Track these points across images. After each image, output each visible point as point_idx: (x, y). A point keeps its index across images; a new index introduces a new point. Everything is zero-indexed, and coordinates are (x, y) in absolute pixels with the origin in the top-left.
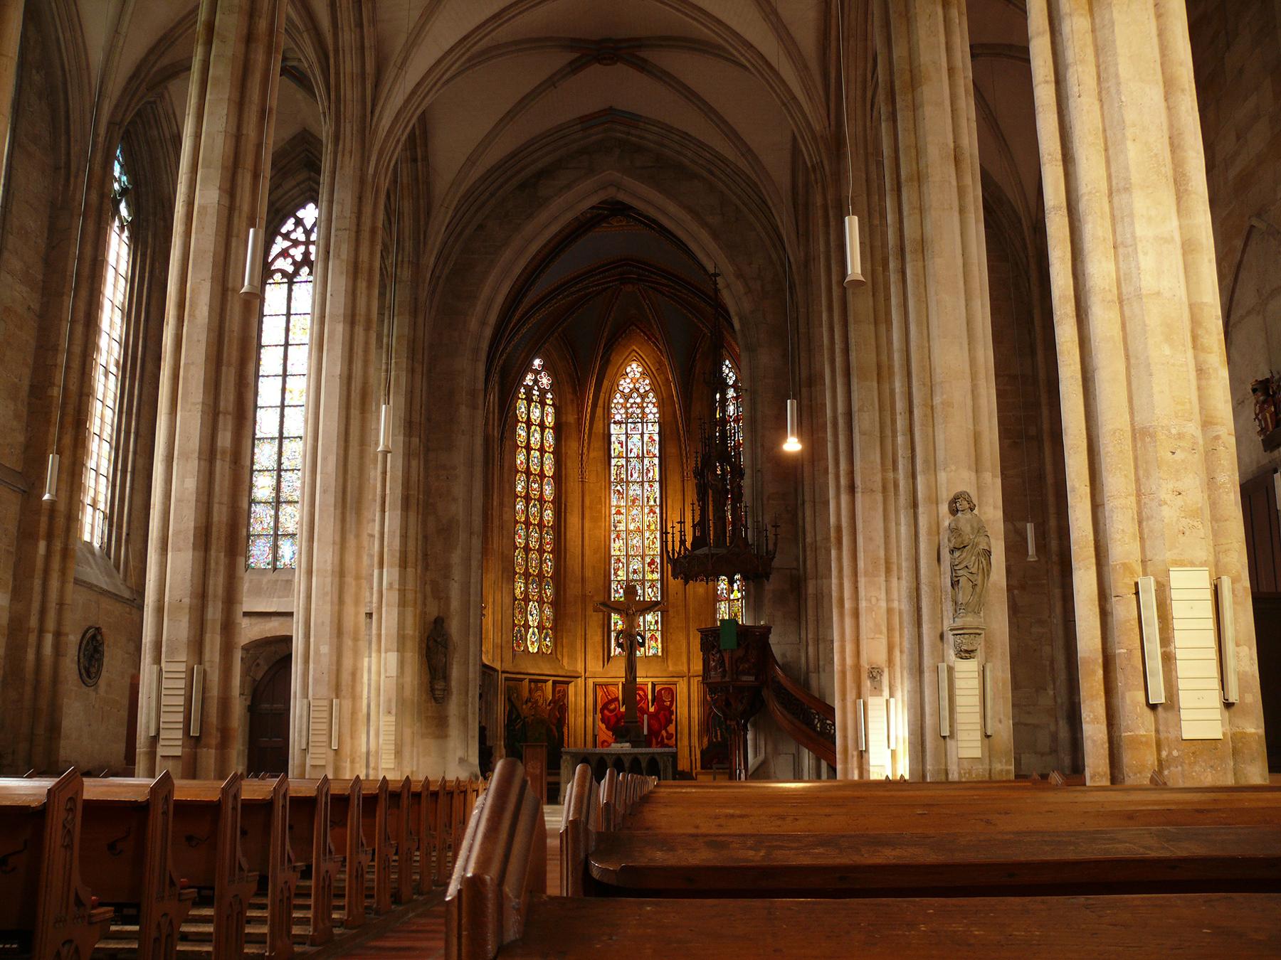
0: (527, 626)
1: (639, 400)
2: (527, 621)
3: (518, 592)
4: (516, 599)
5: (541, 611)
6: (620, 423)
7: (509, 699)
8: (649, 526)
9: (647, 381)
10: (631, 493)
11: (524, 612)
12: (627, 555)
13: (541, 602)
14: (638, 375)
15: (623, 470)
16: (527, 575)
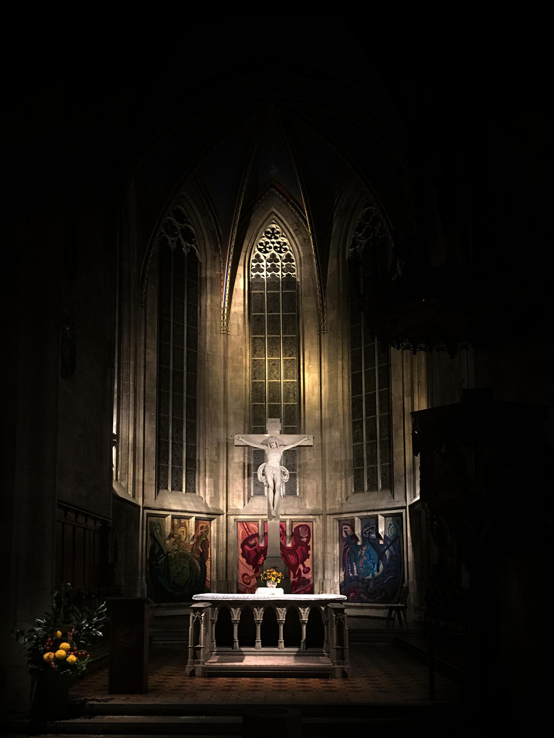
7: (152, 535)
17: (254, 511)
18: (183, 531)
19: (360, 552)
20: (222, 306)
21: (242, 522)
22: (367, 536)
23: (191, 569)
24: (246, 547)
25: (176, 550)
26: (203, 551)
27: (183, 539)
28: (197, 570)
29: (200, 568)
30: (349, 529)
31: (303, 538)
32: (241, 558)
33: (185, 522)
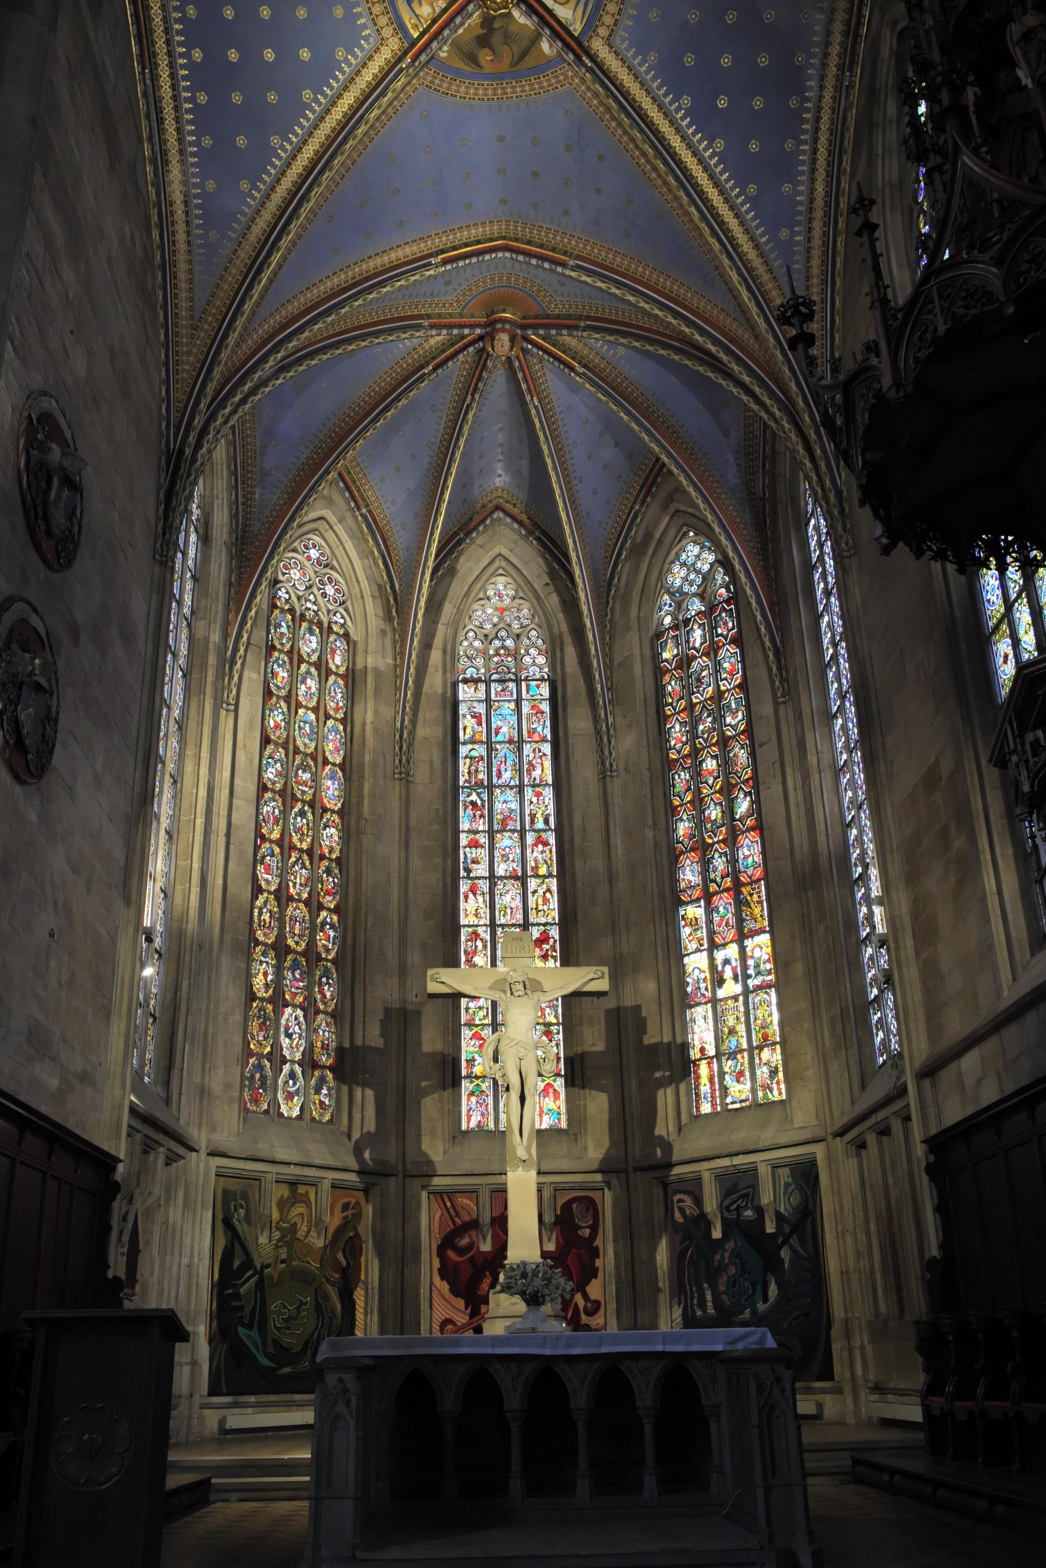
0: (278, 1059)
1: (509, 643)
2: (277, 1046)
3: (259, 982)
4: (252, 997)
5: (311, 1029)
6: (476, 681)
7: (227, 1222)
8: (536, 868)
9: (525, 611)
10: (498, 806)
11: (270, 1024)
12: (493, 925)
13: (310, 1009)
14: (507, 601)
15: (482, 766)
16: (280, 949)
17: (465, 1167)
18: (302, 1215)
19: (718, 1257)
20: (398, 725)
21: (441, 1194)
22: (733, 1216)
23: (318, 1307)
24: (451, 1254)
25: (283, 1261)
26: (348, 1264)
27: (301, 1234)
28: (333, 1311)
29: (339, 1307)
30: (688, 1201)
31: (581, 1228)
32: (437, 1280)
33: (307, 1193)
